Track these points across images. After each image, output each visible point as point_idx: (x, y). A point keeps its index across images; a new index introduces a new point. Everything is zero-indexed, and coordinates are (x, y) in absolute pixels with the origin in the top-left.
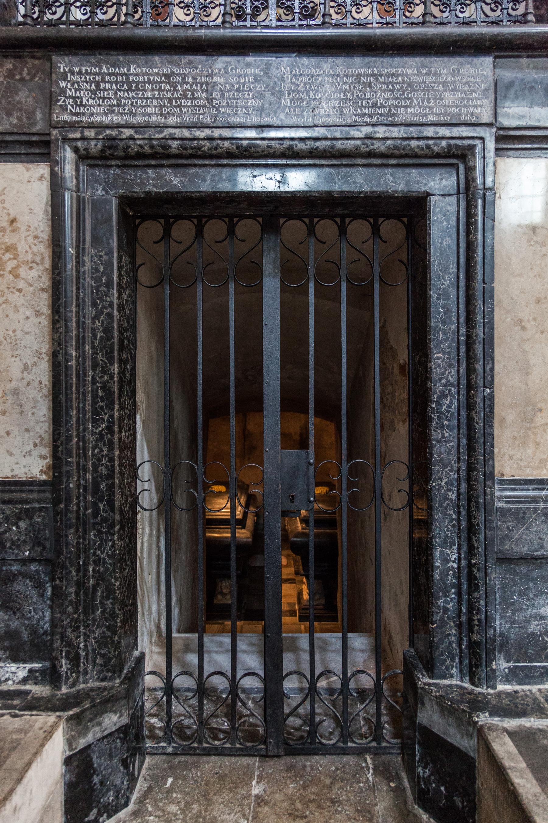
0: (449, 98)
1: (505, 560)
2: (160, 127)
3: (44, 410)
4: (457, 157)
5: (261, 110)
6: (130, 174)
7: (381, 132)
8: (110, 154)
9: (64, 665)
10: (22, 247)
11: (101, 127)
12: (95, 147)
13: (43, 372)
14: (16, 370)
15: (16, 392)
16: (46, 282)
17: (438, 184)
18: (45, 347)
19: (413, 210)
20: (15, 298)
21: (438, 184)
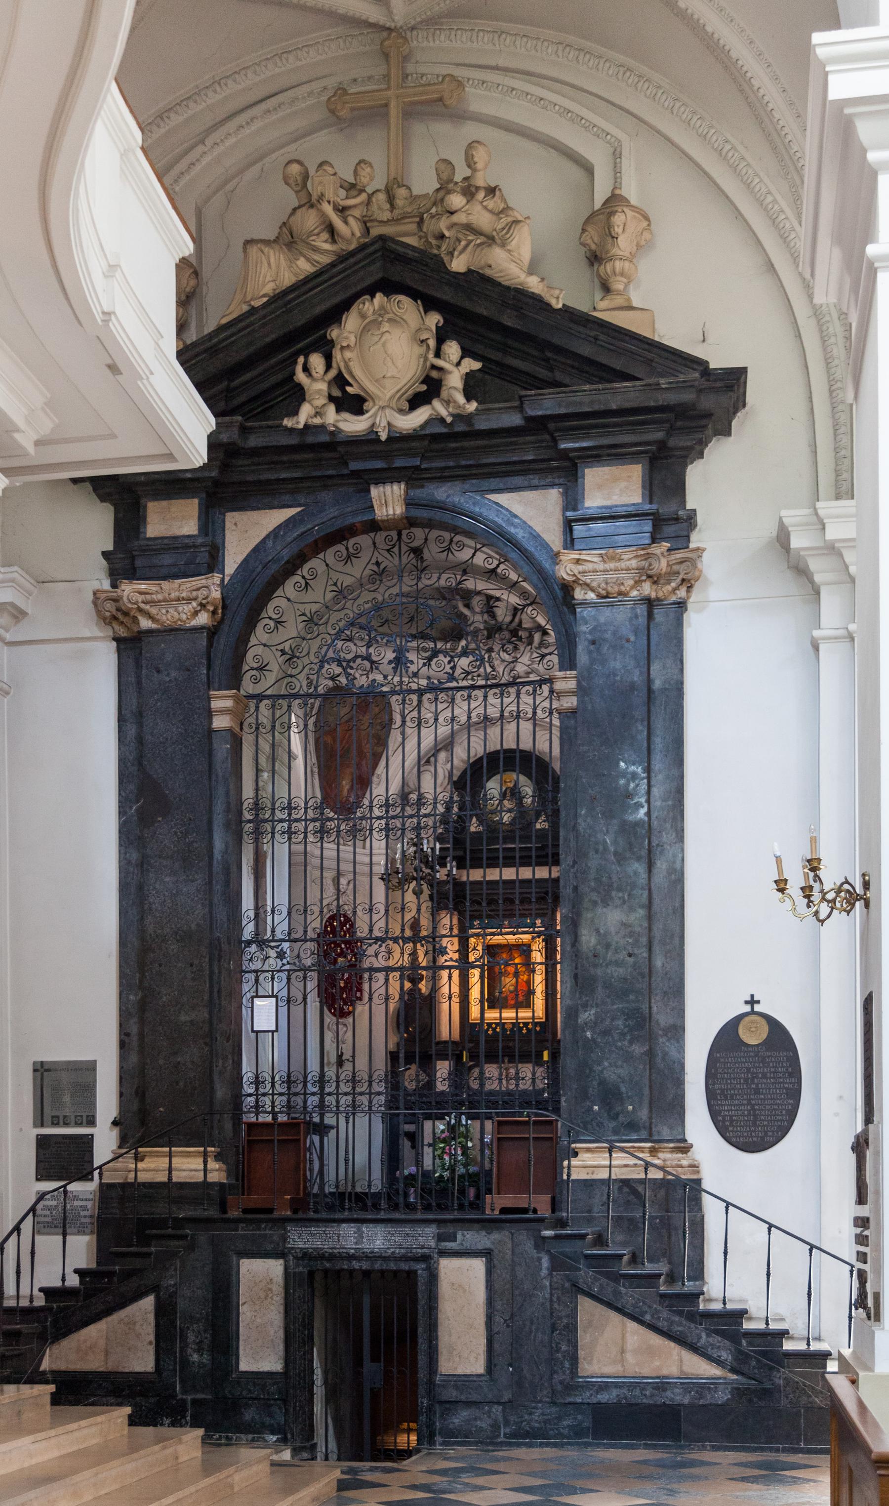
0: (421, 1239)
1: (441, 1403)
2: (321, 1249)
3: (281, 1347)
4: (425, 1258)
5: (356, 1243)
6: (311, 1263)
7: (397, 1251)
8: (305, 1256)
9: (289, 1436)
10: (274, 1289)
11: (301, 1249)
12: (300, 1255)
13: (281, 1334)
14: (272, 1333)
15: (272, 1340)
16: (282, 1301)
17: (420, 1267)
18: (282, 1325)
19: (411, 1275)
20: (272, 1307)
21: (420, 1267)
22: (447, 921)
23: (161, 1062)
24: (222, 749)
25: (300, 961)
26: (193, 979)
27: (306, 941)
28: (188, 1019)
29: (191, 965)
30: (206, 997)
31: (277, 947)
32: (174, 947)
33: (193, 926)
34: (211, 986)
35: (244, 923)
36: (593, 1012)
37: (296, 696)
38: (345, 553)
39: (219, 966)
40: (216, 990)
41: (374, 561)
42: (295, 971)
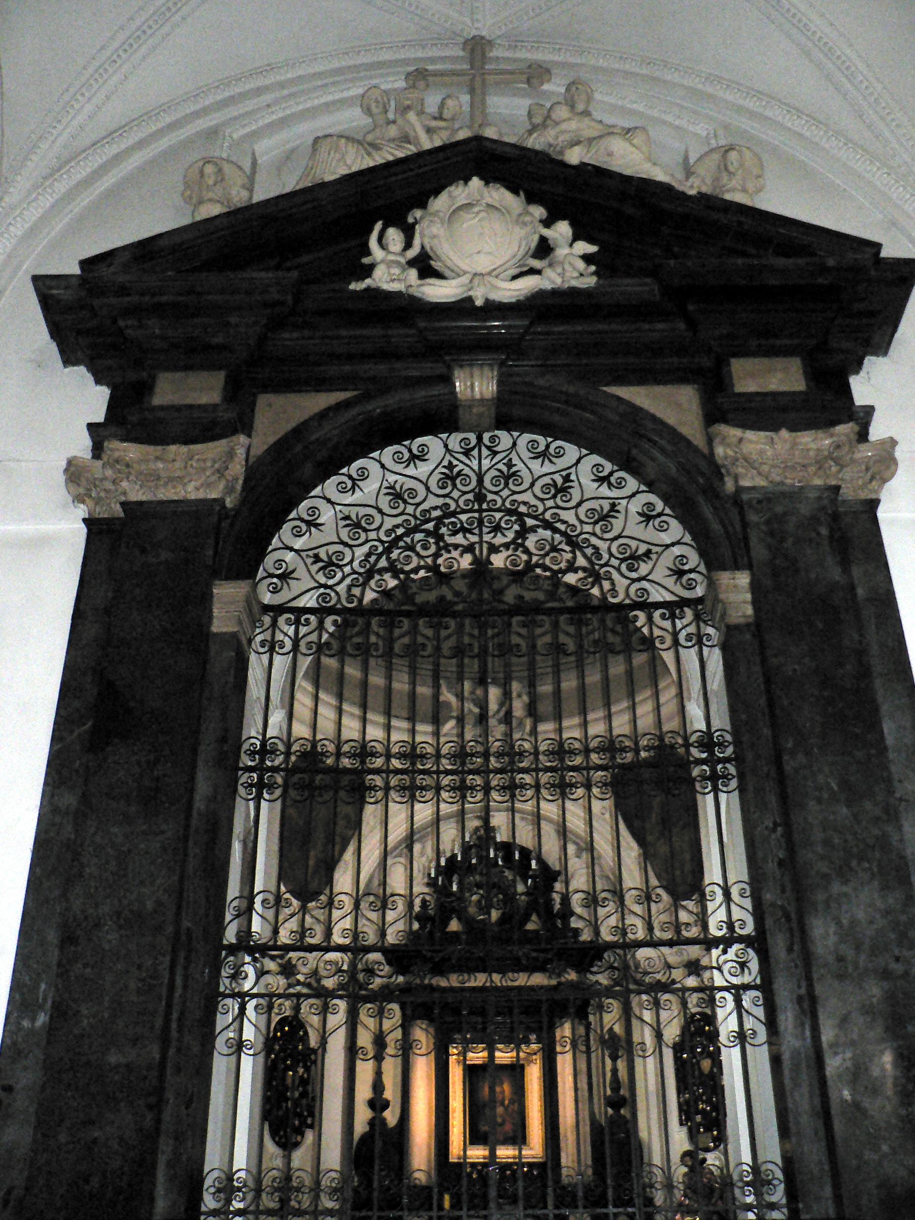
22: (422, 1036)
23: (63, 1138)
24: (220, 659)
25: (318, 981)
26: (139, 992)
27: (327, 950)
28: (123, 1060)
29: (139, 967)
30: (159, 1022)
31: (282, 957)
32: (110, 937)
33: (150, 905)
34: (169, 1006)
35: (228, 917)
36: (849, 1055)
37: (331, 611)
38: (407, 455)
39: (186, 978)
40: (175, 1016)
41: (445, 463)
42: (308, 996)
